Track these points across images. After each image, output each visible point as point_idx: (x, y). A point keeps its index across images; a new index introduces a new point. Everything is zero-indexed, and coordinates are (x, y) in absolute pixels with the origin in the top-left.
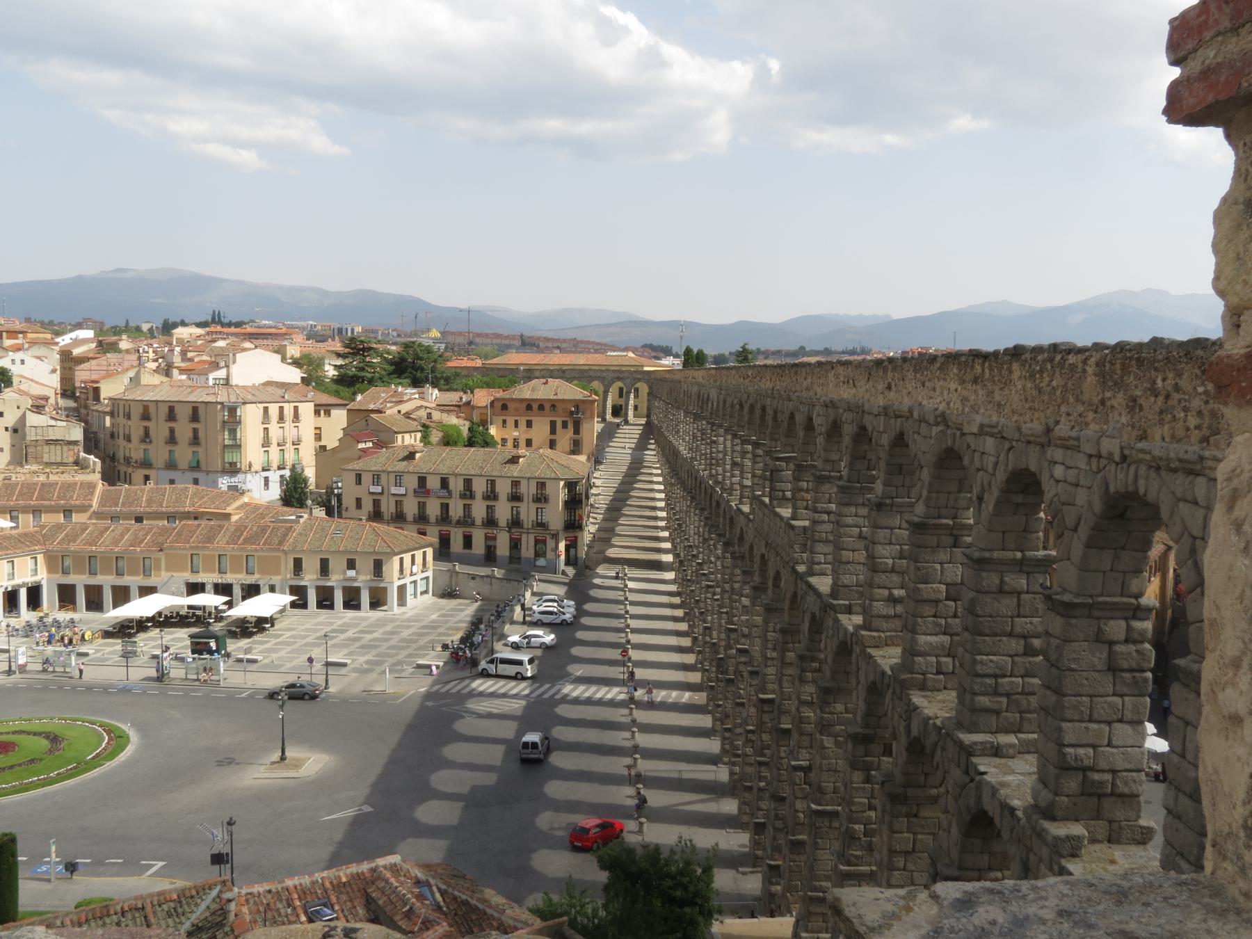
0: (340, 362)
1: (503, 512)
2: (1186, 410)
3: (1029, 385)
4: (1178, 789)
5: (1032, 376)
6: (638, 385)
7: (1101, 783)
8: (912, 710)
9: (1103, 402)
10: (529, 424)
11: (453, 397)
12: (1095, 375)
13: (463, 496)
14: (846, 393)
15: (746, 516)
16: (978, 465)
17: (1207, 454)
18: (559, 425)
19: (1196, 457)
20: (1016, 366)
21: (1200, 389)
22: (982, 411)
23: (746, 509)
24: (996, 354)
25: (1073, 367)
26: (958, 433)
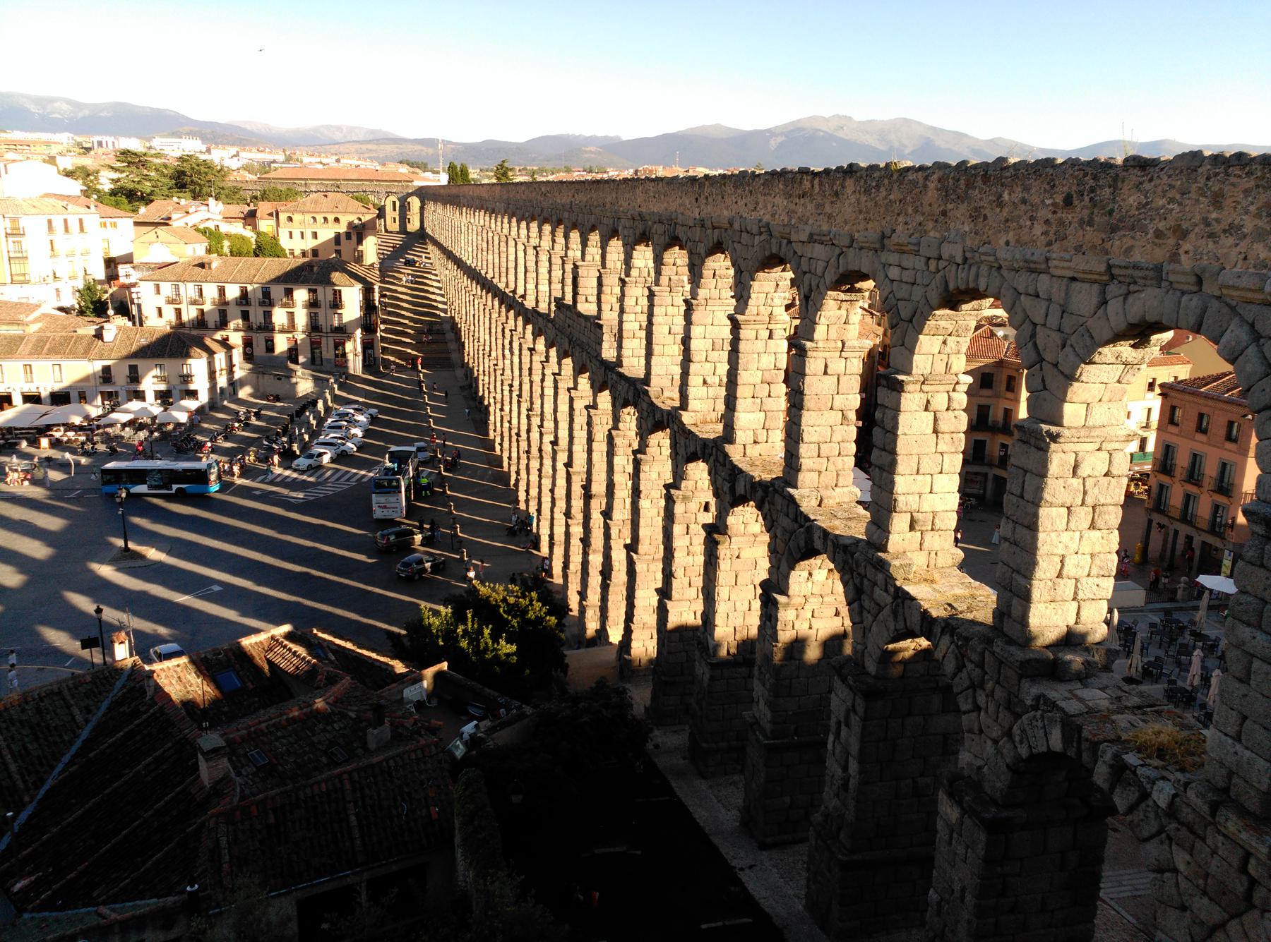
0: (115, 175)
2: (1032, 219)
3: (863, 198)
4: (1015, 522)
5: (867, 191)
9: (944, 213)
10: (315, 235)
12: (938, 190)
13: (262, 304)
14: (657, 207)
16: (805, 268)
17: (1054, 256)
19: (1042, 258)
20: (850, 183)
21: (1048, 202)
22: (811, 221)
25: (914, 183)
26: (785, 242)
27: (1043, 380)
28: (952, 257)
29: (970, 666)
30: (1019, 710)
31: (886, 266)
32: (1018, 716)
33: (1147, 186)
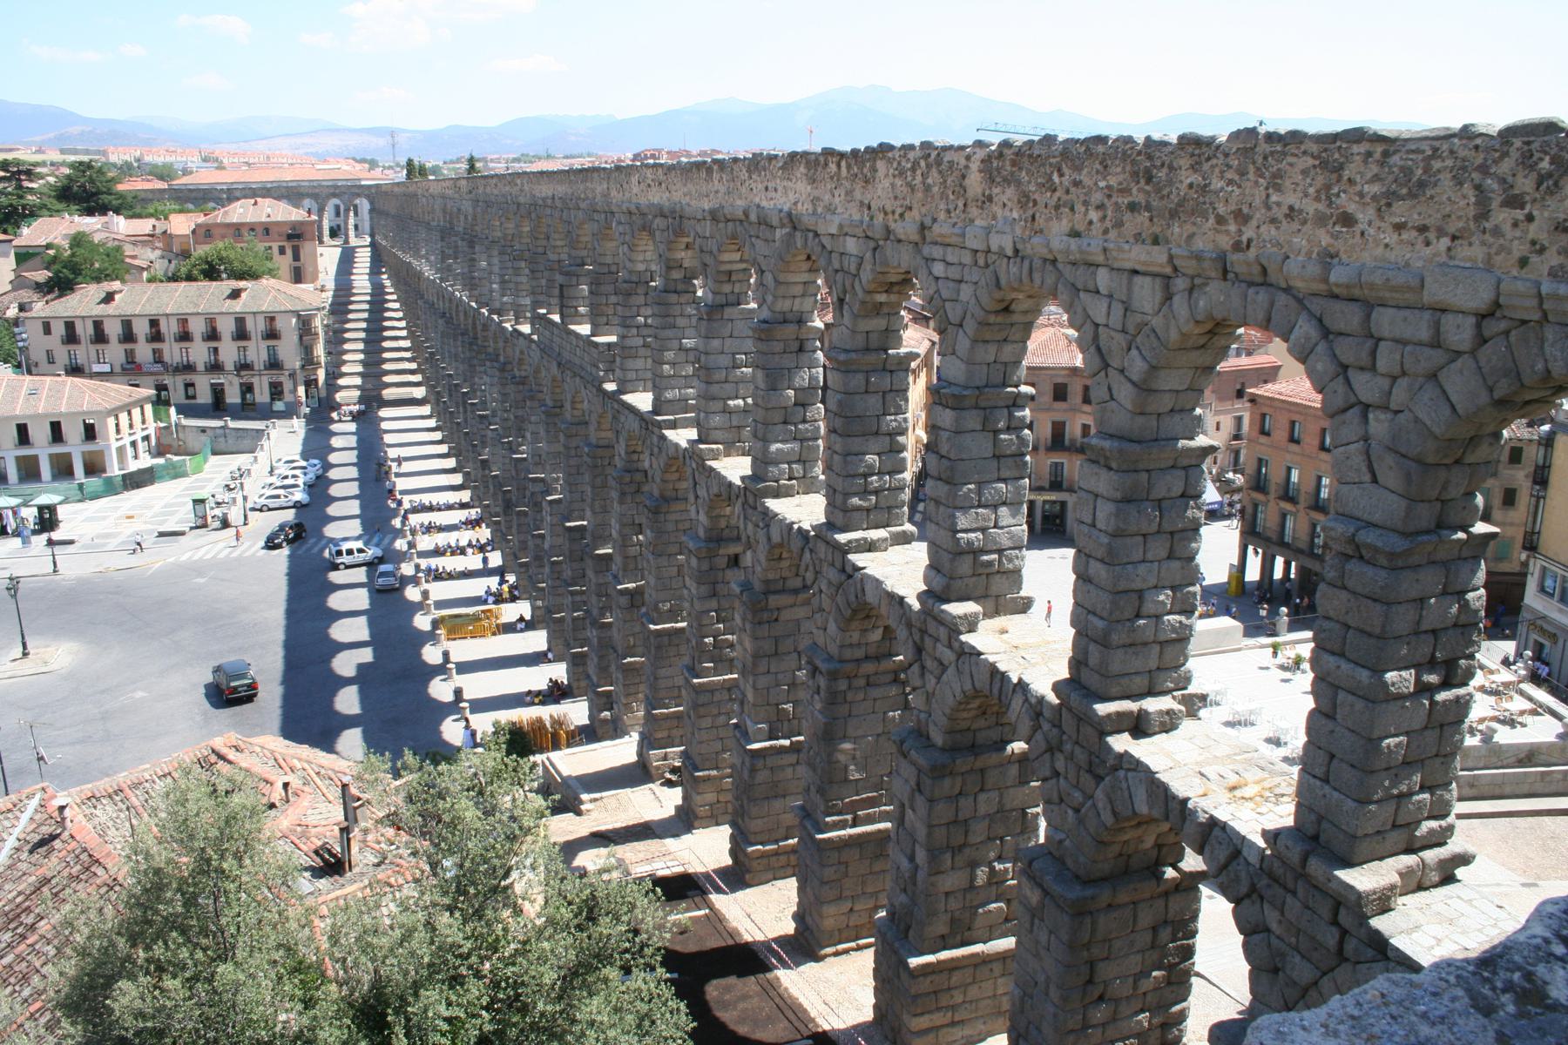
1: (257, 352)
2: (1086, 203)
3: (899, 182)
5: (901, 173)
6: (357, 201)
7: (990, 563)
8: (769, 517)
11: (144, 226)
12: (980, 171)
14: (656, 197)
15: (527, 337)
18: (276, 250)
21: (1102, 184)
23: (526, 329)
24: (855, 152)
26: (811, 235)
27: (1110, 389)
28: (1001, 248)
29: (1046, 726)
30: (1101, 771)
31: (929, 260)
32: (1099, 779)
33: (1206, 166)
